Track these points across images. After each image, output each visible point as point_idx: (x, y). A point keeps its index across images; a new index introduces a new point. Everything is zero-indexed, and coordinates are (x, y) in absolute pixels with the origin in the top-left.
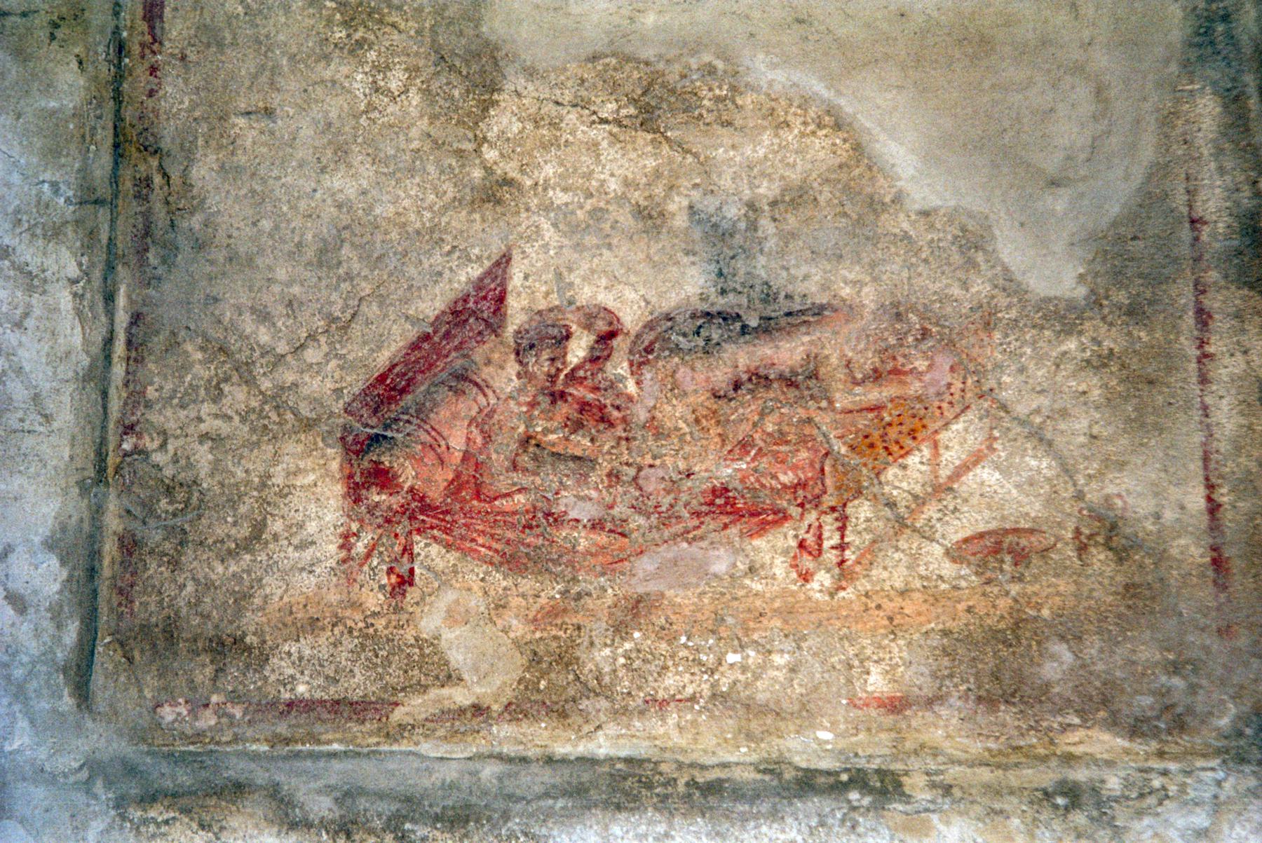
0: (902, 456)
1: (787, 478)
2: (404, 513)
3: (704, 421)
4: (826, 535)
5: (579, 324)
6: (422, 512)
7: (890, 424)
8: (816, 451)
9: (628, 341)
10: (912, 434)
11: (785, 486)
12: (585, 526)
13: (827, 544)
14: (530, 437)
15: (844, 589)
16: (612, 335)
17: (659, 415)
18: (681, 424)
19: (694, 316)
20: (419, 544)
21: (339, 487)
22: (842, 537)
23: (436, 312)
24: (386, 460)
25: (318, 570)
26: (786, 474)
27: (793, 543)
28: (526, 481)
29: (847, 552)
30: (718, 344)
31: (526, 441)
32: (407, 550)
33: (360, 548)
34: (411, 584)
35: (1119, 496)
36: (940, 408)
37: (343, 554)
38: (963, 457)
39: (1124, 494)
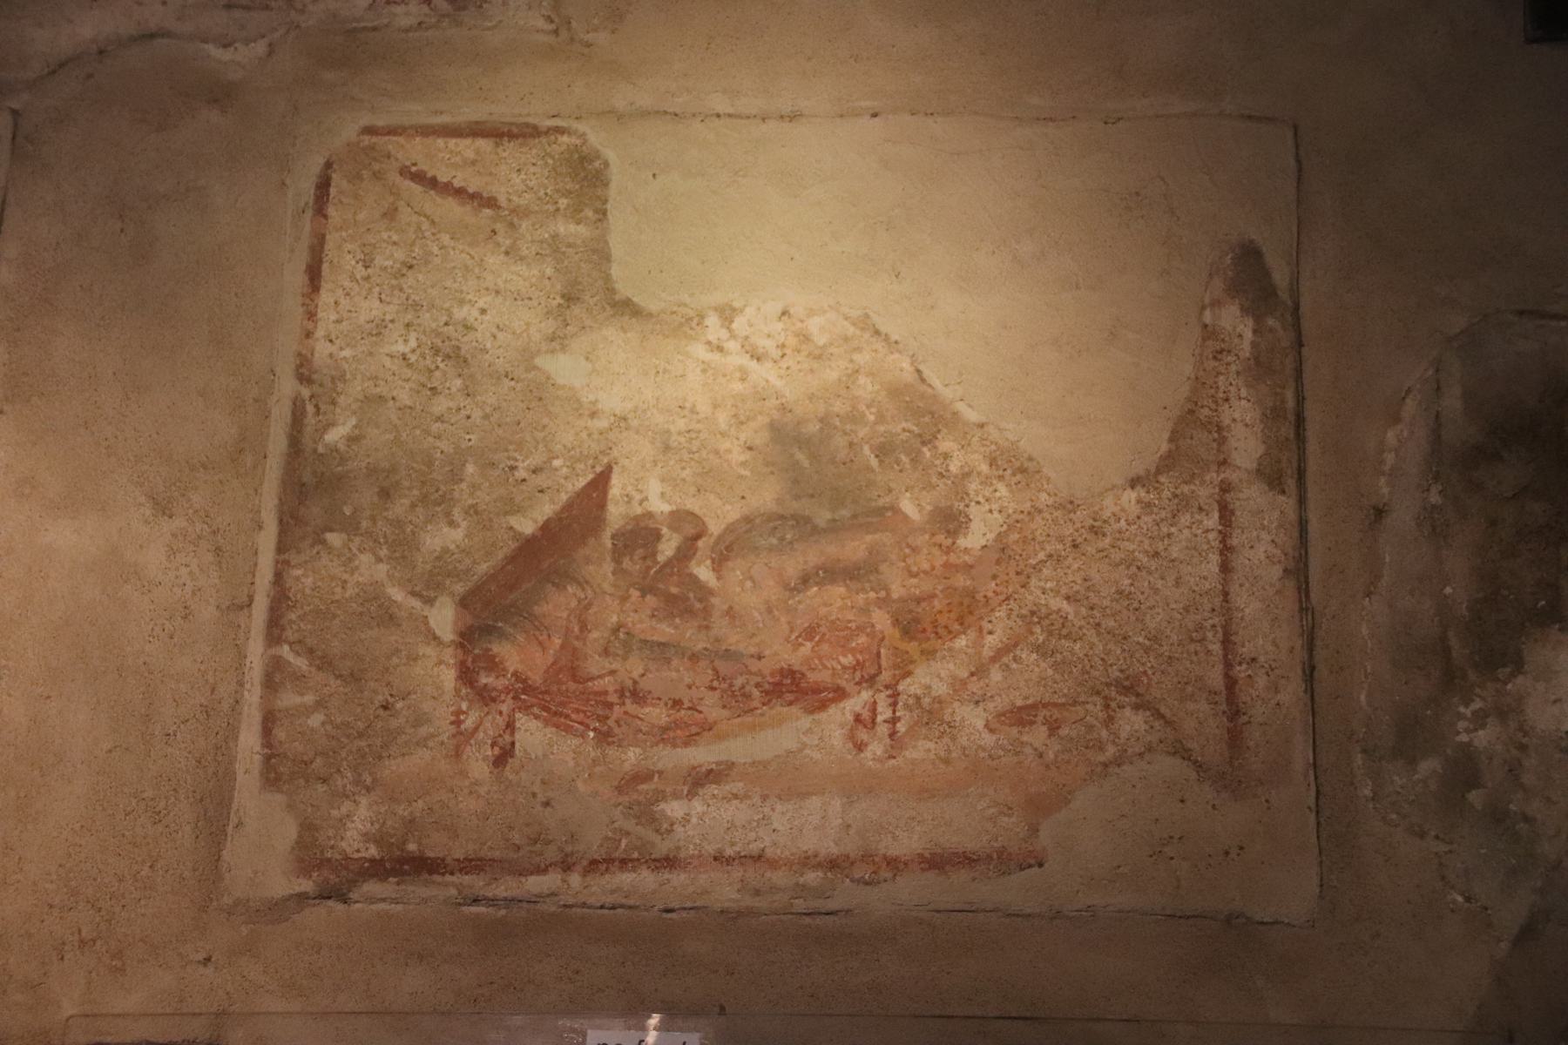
1: (848, 660)
4: (880, 709)
5: (670, 527)
11: (844, 668)
13: (880, 719)
16: (698, 537)
19: (769, 520)
20: (522, 720)
25: (431, 744)
27: (850, 718)
31: (616, 630)
32: (510, 726)
33: (469, 723)
37: (453, 729)
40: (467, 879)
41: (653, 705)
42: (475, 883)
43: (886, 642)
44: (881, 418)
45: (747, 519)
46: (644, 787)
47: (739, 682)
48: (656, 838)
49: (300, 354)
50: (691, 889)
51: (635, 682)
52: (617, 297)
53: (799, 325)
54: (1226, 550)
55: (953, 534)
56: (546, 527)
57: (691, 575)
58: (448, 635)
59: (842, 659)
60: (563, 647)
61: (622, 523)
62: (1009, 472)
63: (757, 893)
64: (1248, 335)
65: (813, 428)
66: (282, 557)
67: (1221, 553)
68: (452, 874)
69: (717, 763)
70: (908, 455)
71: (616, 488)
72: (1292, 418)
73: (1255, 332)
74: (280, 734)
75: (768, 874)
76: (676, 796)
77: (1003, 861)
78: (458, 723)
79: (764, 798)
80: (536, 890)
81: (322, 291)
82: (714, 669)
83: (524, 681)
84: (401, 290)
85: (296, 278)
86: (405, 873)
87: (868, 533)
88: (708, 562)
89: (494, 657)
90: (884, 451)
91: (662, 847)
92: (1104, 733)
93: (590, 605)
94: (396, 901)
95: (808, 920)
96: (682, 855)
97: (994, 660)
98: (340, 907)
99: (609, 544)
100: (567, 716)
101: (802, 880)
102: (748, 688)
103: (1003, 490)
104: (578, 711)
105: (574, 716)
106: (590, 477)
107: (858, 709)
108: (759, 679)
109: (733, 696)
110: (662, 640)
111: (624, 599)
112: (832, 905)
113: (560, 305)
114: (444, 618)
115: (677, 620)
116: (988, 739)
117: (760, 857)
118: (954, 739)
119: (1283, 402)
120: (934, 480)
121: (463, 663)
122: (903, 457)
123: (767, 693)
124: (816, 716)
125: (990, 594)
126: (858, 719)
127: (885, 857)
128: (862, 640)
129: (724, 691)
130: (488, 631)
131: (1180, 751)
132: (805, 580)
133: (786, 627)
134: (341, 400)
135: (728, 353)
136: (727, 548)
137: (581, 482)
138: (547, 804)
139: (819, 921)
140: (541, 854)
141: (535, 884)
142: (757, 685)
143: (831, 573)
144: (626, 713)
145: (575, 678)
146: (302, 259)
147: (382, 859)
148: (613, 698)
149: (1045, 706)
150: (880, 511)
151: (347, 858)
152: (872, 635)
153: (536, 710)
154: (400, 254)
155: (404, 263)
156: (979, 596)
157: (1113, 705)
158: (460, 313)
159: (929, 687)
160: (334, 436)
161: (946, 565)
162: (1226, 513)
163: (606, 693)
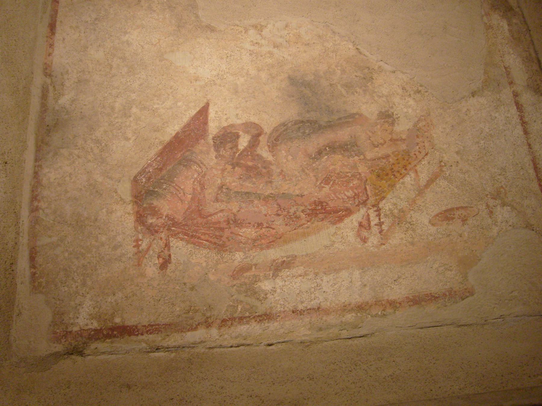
0: (402, 178)
1: (350, 193)
2: (164, 227)
3: (306, 170)
4: (371, 218)
6: (173, 225)
7: (394, 164)
8: (361, 180)
9: (267, 136)
10: (405, 167)
11: (348, 197)
12: (254, 226)
13: (373, 223)
14: (223, 185)
15: (384, 244)
16: (259, 135)
17: (284, 170)
18: (296, 173)
20: (174, 242)
21: (133, 217)
22: (380, 219)
23: (176, 132)
24: (155, 203)
25: (124, 259)
26: (348, 191)
27: (356, 224)
28: (223, 206)
29: (383, 226)
30: (309, 134)
31: (221, 188)
32: (167, 245)
33: (144, 245)
34: (170, 263)
35: (502, 187)
36: (415, 154)
37: (135, 250)
38: (430, 176)
39: (504, 186)
40: (151, 337)
41: (247, 227)
42: (156, 338)
43: (368, 182)
44: (343, 71)
45: (284, 124)
46: (248, 274)
47: (292, 211)
48: (258, 304)
49: (46, 64)
50: (282, 331)
51: (235, 215)
52: (203, 24)
53: (295, 31)
54: (524, 123)
55: (393, 124)
56: (176, 136)
57: (258, 155)
58: (128, 198)
59: (346, 193)
60: (192, 199)
61: (217, 131)
62: (412, 93)
63: (320, 329)
64: (506, 27)
65: (310, 78)
66: (37, 164)
67: (522, 125)
68: (142, 334)
69: (288, 257)
70: (361, 88)
71: (212, 113)
72: (536, 61)
73: (508, 25)
74: (39, 260)
75: (324, 318)
76: (266, 277)
77: (451, 296)
78: (137, 246)
79: (316, 274)
80: (192, 340)
81: (57, 35)
82: (278, 204)
83: (173, 219)
84: (95, 30)
85: (43, 29)
86: (115, 336)
87: (348, 127)
88: (266, 148)
89: (155, 207)
90: (348, 86)
91: (262, 309)
92: (490, 221)
93: (205, 174)
94: (111, 353)
95: (350, 342)
96: (274, 312)
97: (427, 186)
98: (79, 358)
99: (211, 142)
100: (199, 238)
101: (344, 319)
102: (298, 213)
103: (411, 102)
104: (205, 234)
105: (203, 237)
106: (198, 109)
107: (360, 219)
108: (303, 208)
109: (291, 218)
110: (246, 191)
111: (223, 170)
112: (363, 332)
113: (174, 30)
114: (125, 189)
115: (254, 180)
116: (433, 229)
117: (319, 308)
118: (414, 230)
119: (530, 55)
120: (376, 98)
121: (138, 212)
122: (358, 90)
123: (309, 215)
124: (338, 226)
125: (417, 153)
126: (361, 225)
127: (388, 301)
128: (356, 182)
129: (285, 216)
130: (150, 193)
131: (529, 226)
132: (320, 153)
133: (313, 178)
134: (67, 84)
135: (261, 46)
136: (275, 140)
137: (193, 112)
138: (192, 289)
139: (356, 341)
140: (192, 318)
141: (190, 337)
142: (303, 211)
143: (333, 148)
144: (232, 233)
145: (201, 216)
146: (47, 20)
147: (101, 329)
148: (223, 225)
149: (457, 209)
150: (352, 116)
151: (81, 330)
152: (360, 179)
153: (181, 235)
154: (94, 16)
155: (96, 19)
156: (412, 154)
157: (491, 205)
158: (125, 38)
159: (395, 204)
160: (64, 100)
161: (391, 140)
162: (519, 107)
163: (219, 222)
